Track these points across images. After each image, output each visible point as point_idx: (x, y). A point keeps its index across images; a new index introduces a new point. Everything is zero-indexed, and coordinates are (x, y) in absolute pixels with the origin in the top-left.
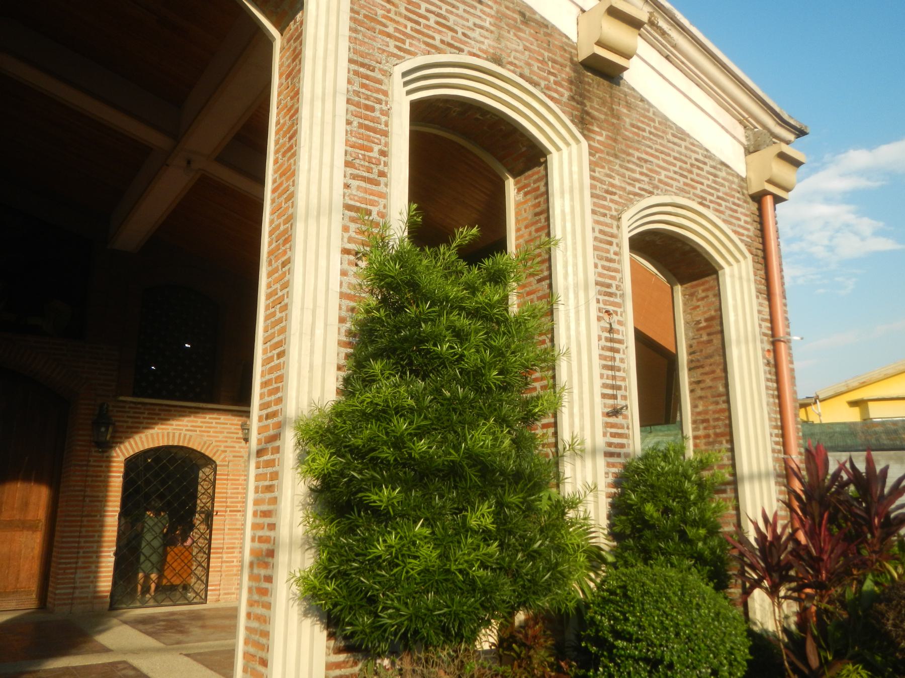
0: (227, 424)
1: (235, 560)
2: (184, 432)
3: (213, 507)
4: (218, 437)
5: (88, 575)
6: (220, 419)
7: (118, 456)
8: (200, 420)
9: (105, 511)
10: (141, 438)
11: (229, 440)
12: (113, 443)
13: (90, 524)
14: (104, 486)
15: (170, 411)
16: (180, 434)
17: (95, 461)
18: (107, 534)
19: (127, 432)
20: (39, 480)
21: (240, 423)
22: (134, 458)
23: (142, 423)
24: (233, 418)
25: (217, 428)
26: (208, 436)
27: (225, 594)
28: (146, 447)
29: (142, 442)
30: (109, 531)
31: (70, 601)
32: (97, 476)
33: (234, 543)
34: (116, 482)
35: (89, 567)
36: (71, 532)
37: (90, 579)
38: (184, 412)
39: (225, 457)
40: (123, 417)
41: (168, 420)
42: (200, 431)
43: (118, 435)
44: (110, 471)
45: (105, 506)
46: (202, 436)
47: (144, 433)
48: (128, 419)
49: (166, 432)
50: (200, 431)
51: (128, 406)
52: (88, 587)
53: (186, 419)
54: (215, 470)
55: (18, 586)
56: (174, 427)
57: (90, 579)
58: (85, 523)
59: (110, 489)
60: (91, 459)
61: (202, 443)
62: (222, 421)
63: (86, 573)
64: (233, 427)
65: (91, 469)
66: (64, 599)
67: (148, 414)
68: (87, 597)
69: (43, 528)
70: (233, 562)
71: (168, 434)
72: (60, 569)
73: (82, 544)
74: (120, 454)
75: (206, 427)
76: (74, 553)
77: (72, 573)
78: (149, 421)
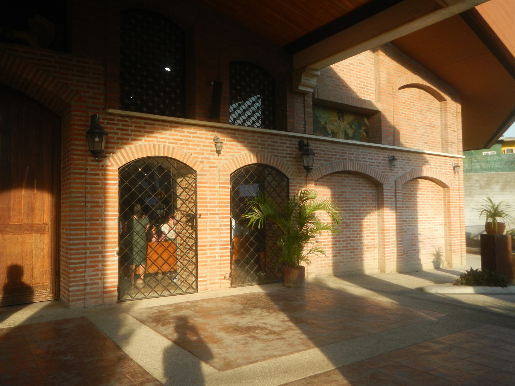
0: (202, 138)
1: (217, 255)
2: (167, 145)
3: (196, 210)
4: (196, 149)
5: (96, 273)
6: (196, 133)
7: (112, 165)
8: (180, 134)
9: (105, 216)
10: (131, 149)
11: (205, 152)
12: (107, 153)
13: (93, 227)
14: (102, 193)
15: (154, 125)
16: (164, 146)
17: (91, 170)
18: (109, 236)
19: (118, 143)
20: (41, 187)
21: (213, 137)
22: (127, 167)
23: (130, 135)
24: (207, 132)
25: (194, 141)
26: (187, 148)
27: (211, 284)
28: (137, 157)
29: (133, 153)
30: (111, 233)
31: (83, 297)
32: (95, 184)
33: (215, 241)
34: (112, 189)
35: (97, 266)
36: (77, 235)
37: (99, 276)
38: (167, 126)
39: (203, 167)
40: (113, 129)
41: (153, 133)
42: (181, 144)
43: (110, 145)
44: (106, 179)
45: (105, 211)
46: (183, 148)
47: (133, 144)
48: (118, 131)
49: (152, 144)
50: (181, 144)
51: (117, 118)
52: (98, 283)
53: (168, 132)
54: (196, 179)
55: (33, 281)
56: (158, 139)
57: (99, 276)
58: (89, 227)
59: (108, 195)
60: (88, 167)
61: (184, 155)
62: (198, 135)
63: (94, 271)
64: (207, 141)
65: (89, 177)
66: (77, 295)
67: (136, 127)
68: (98, 292)
69: (50, 230)
70: (215, 257)
71: (154, 145)
72: (70, 268)
73: (88, 246)
74: (114, 163)
75: (185, 140)
76: (82, 254)
77: (82, 272)
78: (136, 133)
